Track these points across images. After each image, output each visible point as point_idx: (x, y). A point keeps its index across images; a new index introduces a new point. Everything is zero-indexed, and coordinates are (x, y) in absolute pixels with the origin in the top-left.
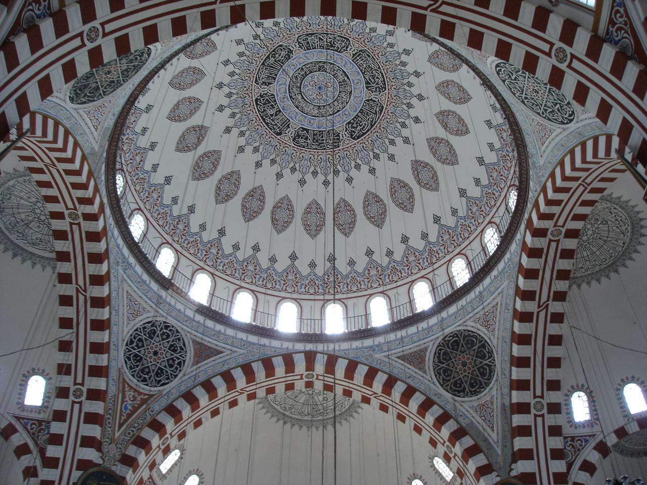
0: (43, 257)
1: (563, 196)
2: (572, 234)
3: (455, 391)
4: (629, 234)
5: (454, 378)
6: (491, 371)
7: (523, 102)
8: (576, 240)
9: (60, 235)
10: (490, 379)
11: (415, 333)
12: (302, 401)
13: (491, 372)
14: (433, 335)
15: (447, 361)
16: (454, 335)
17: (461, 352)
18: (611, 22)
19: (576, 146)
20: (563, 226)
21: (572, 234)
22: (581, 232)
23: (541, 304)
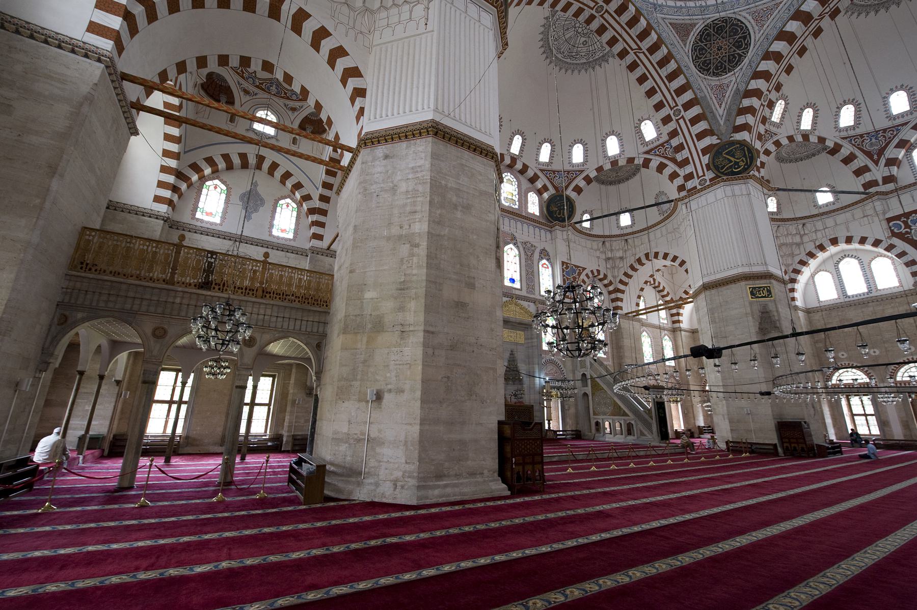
3: (701, 68)
5: (706, 57)
10: (734, 67)
11: (693, 7)
12: (567, 37)
14: (707, 14)
15: (707, 41)
16: (725, 20)
17: (722, 37)
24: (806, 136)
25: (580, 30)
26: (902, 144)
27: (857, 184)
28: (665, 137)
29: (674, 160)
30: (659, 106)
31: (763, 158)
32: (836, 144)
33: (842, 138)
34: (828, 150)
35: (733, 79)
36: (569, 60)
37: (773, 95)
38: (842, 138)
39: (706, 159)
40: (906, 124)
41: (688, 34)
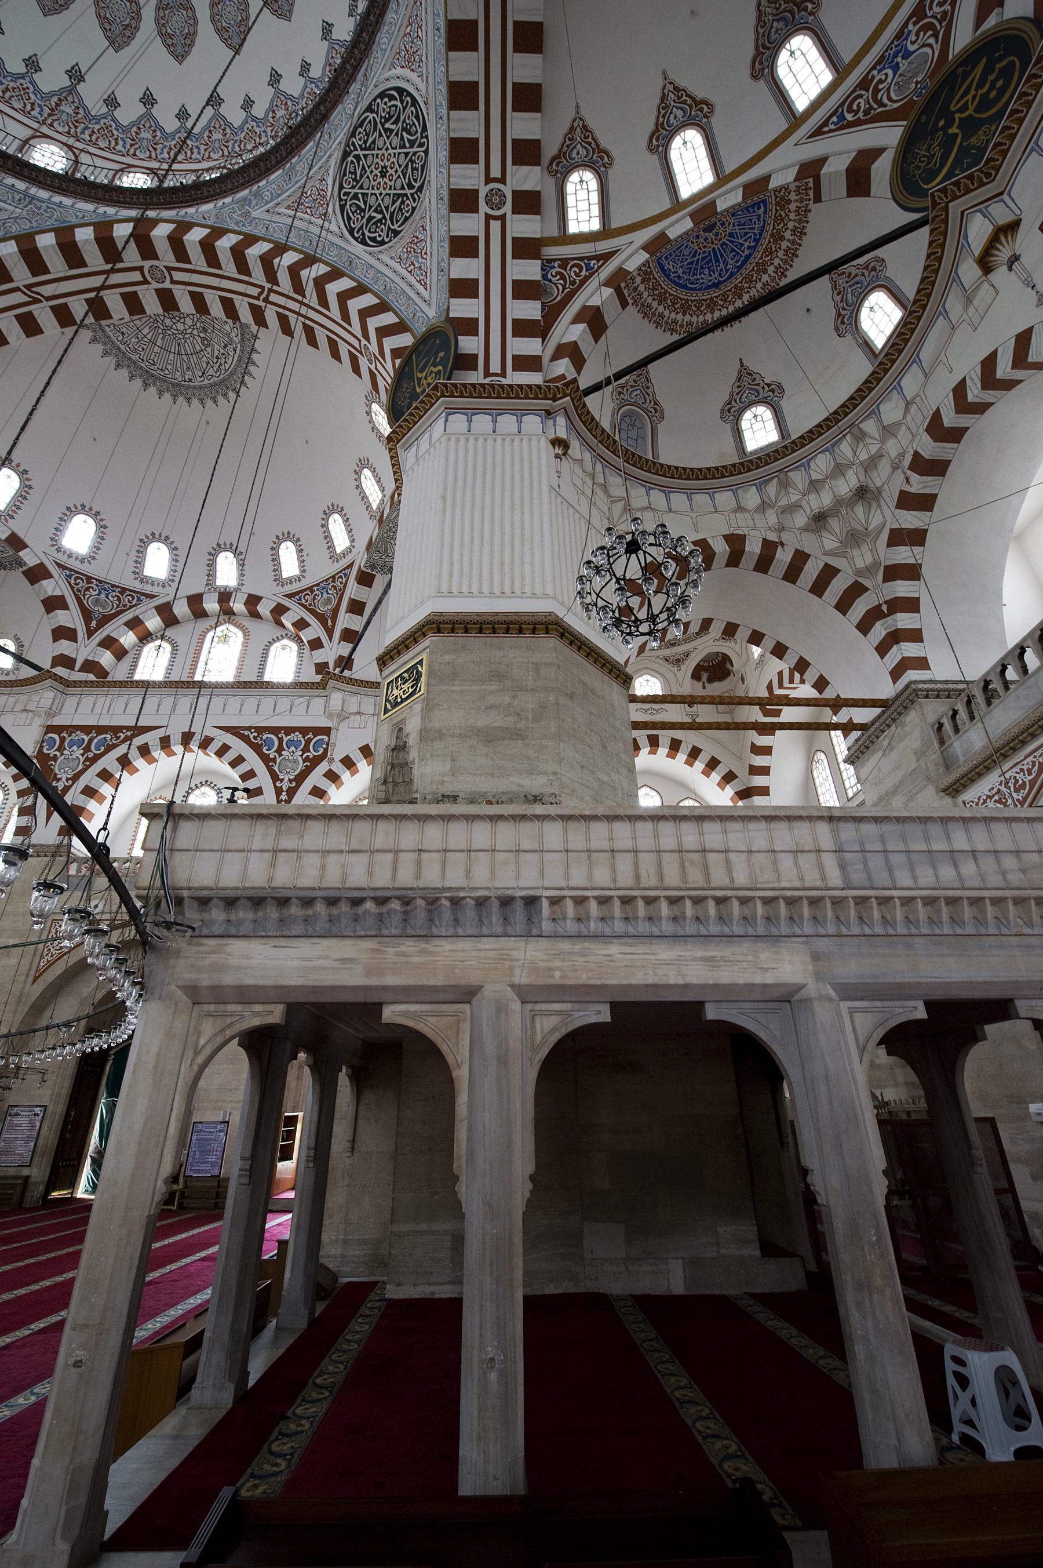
1: (229, 267)
2: (167, 300)
4: (206, 382)
7: (346, 155)
8: (160, 311)
18: (564, 262)
19: (326, 263)
20: (173, 282)
21: (167, 300)
22: (177, 313)
23: (34, 289)
26: (134, 624)
27: (44, 653)
33: (59, 565)
34: (25, 568)
38: (59, 565)
40: (152, 597)
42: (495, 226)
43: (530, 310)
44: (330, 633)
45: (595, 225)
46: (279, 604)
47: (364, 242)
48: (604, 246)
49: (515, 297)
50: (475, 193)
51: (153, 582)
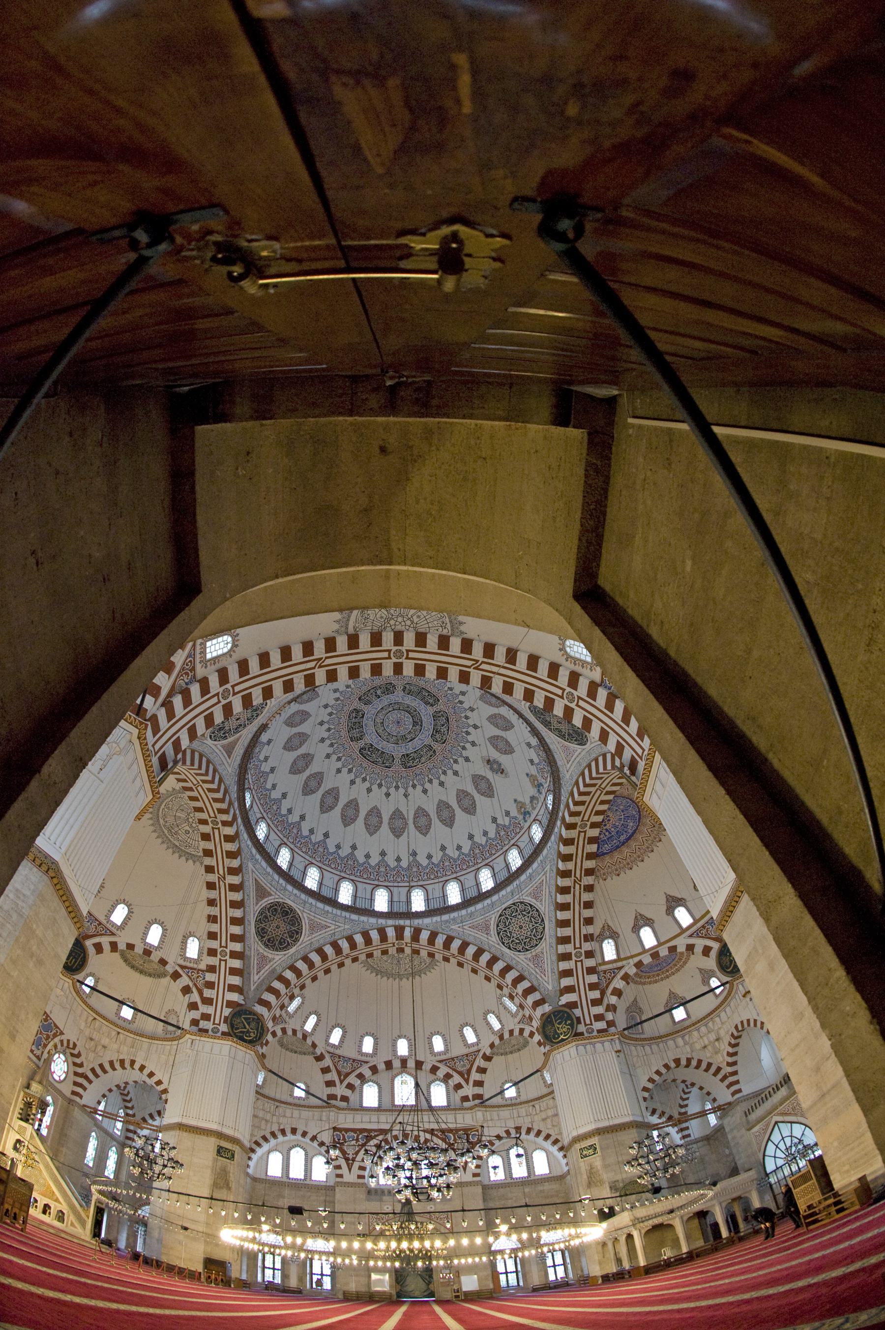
0: (348, 620)
2: (401, 950)
6: (286, 947)
9: (376, 639)
10: (281, 949)
12: (178, 814)
13: (288, 946)
18: (605, 972)
24: (305, 1036)
25: (191, 820)
28: (203, 966)
29: (201, 993)
30: (212, 936)
31: (269, 1037)
32: (322, 1053)
35: (278, 959)
36: (166, 832)
37: (296, 991)
39: (227, 1012)
40: (367, 1062)
41: (263, 898)
42: (579, 964)
43: (596, 994)
44: (467, 1081)
45: (615, 957)
46: (434, 1066)
47: (509, 948)
48: (619, 964)
49: (590, 990)
50: (570, 954)
51: (367, 1055)
